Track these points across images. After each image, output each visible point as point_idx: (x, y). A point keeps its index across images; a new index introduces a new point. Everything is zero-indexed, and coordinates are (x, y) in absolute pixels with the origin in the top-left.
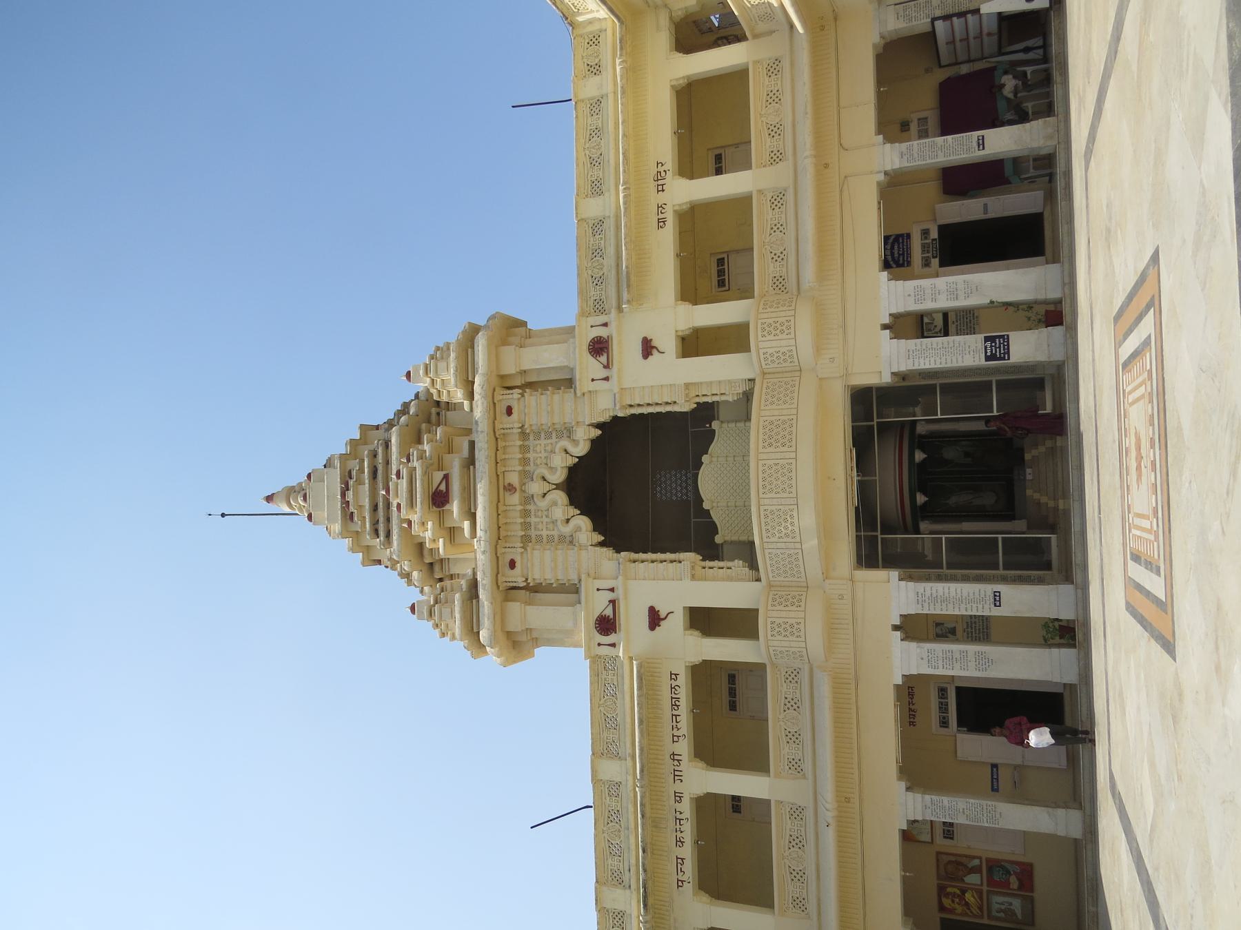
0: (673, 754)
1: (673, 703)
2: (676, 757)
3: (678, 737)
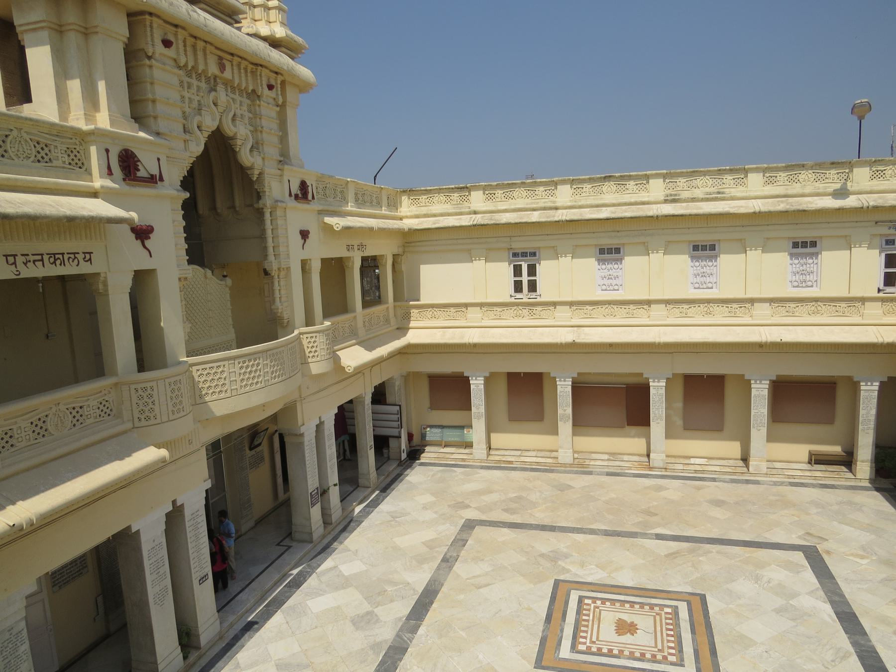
1: (57, 256)
3: (14, 263)
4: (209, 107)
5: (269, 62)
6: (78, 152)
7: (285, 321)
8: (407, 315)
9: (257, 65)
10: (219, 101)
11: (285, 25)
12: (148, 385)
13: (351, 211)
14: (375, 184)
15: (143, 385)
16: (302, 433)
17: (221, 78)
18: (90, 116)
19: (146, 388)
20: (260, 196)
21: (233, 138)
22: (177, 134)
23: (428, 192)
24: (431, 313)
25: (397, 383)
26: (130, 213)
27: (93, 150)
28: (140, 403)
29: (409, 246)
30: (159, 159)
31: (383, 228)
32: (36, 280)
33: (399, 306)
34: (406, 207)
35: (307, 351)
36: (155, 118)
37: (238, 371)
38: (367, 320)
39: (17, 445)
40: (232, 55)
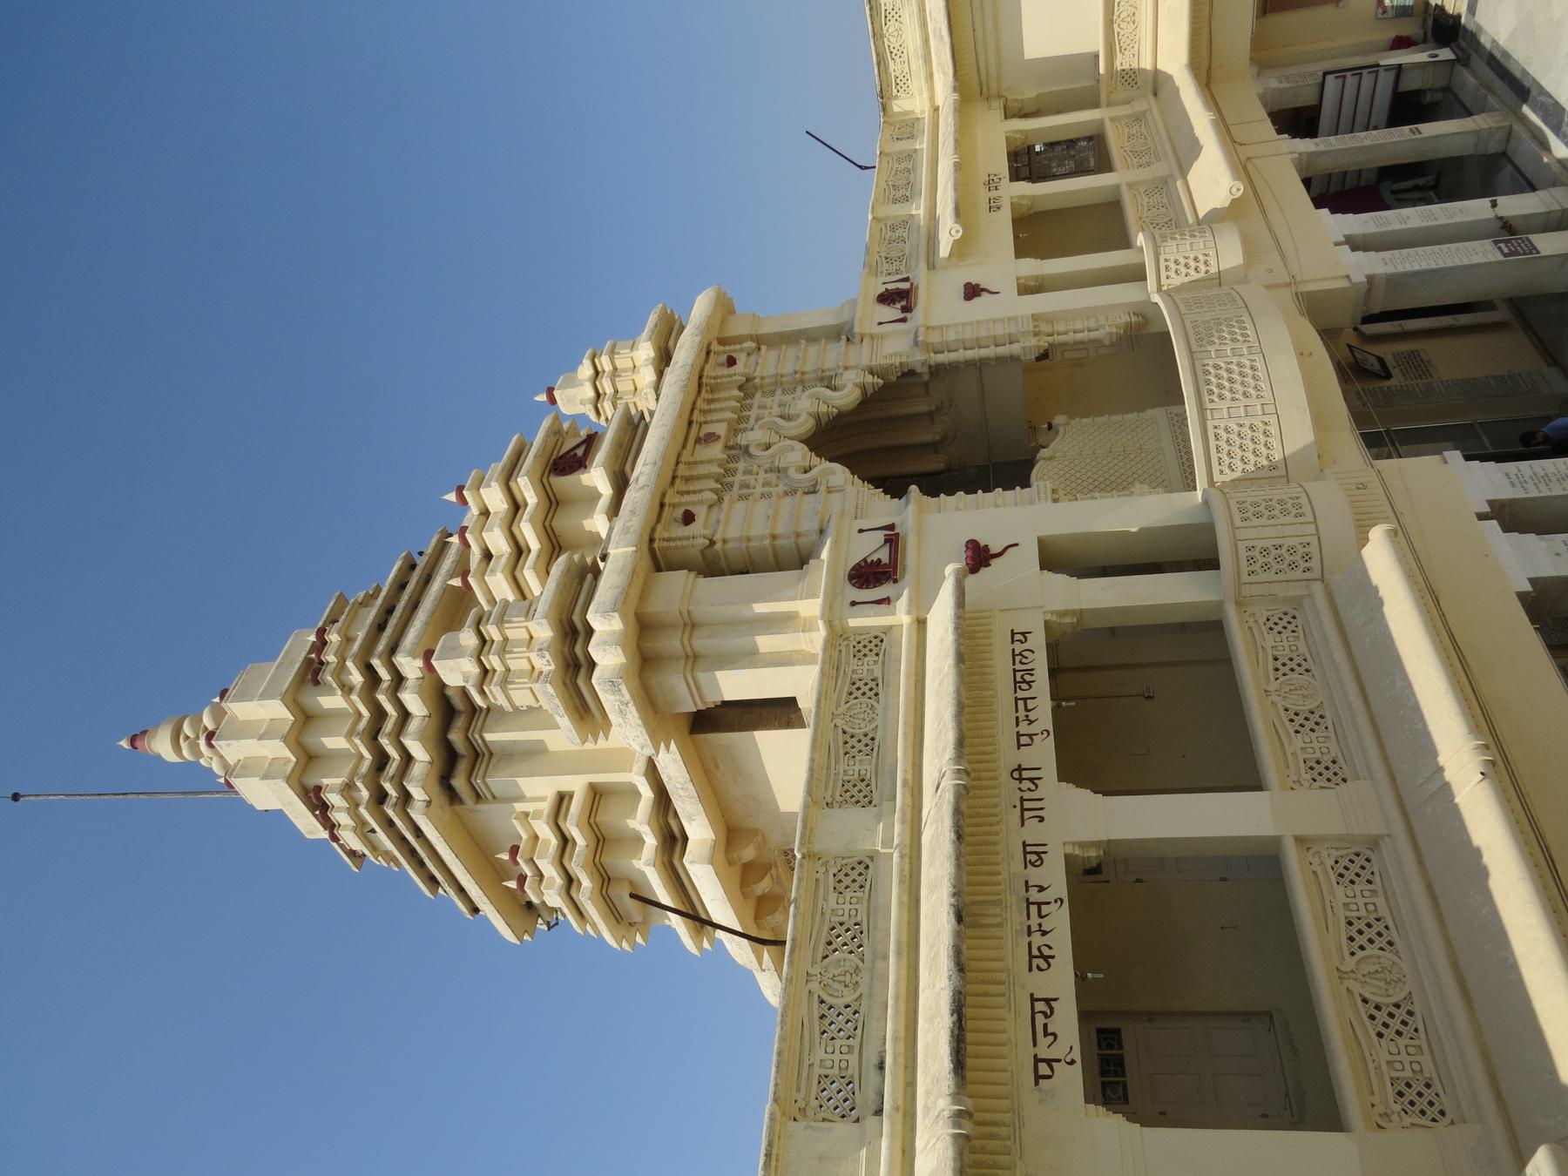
0: (1020, 769)
1: (1019, 679)
2: (1025, 774)
3: (1030, 736)
4: (773, 456)
5: (692, 365)
6: (859, 643)
7: (1133, 320)
8: (1127, 77)
9: (700, 384)
10: (763, 441)
11: (633, 345)
12: (1243, 554)
13: (925, 207)
14: (874, 167)
15: (1243, 562)
16: (1366, 280)
17: (728, 439)
18: (805, 625)
19: (1250, 558)
20: (909, 371)
21: (817, 417)
22: (820, 503)
23: (881, 62)
24: (1123, 25)
25: (1274, 84)
26: (946, 574)
27: (854, 622)
28: (1275, 567)
29: (988, 88)
30: (861, 531)
31: (955, 144)
32: (1056, 710)
33: (1108, 96)
34: (912, 101)
35: (1194, 276)
36: (798, 535)
37: (1228, 403)
38: (1136, 160)
39: (1333, 755)
40: (690, 423)
